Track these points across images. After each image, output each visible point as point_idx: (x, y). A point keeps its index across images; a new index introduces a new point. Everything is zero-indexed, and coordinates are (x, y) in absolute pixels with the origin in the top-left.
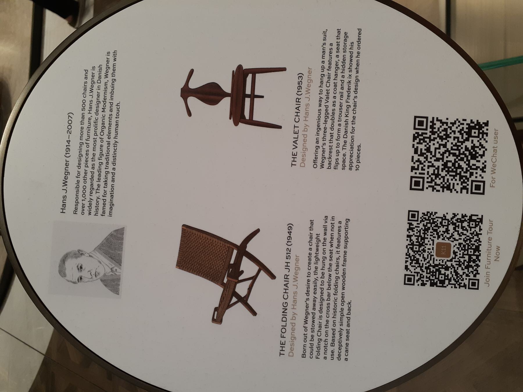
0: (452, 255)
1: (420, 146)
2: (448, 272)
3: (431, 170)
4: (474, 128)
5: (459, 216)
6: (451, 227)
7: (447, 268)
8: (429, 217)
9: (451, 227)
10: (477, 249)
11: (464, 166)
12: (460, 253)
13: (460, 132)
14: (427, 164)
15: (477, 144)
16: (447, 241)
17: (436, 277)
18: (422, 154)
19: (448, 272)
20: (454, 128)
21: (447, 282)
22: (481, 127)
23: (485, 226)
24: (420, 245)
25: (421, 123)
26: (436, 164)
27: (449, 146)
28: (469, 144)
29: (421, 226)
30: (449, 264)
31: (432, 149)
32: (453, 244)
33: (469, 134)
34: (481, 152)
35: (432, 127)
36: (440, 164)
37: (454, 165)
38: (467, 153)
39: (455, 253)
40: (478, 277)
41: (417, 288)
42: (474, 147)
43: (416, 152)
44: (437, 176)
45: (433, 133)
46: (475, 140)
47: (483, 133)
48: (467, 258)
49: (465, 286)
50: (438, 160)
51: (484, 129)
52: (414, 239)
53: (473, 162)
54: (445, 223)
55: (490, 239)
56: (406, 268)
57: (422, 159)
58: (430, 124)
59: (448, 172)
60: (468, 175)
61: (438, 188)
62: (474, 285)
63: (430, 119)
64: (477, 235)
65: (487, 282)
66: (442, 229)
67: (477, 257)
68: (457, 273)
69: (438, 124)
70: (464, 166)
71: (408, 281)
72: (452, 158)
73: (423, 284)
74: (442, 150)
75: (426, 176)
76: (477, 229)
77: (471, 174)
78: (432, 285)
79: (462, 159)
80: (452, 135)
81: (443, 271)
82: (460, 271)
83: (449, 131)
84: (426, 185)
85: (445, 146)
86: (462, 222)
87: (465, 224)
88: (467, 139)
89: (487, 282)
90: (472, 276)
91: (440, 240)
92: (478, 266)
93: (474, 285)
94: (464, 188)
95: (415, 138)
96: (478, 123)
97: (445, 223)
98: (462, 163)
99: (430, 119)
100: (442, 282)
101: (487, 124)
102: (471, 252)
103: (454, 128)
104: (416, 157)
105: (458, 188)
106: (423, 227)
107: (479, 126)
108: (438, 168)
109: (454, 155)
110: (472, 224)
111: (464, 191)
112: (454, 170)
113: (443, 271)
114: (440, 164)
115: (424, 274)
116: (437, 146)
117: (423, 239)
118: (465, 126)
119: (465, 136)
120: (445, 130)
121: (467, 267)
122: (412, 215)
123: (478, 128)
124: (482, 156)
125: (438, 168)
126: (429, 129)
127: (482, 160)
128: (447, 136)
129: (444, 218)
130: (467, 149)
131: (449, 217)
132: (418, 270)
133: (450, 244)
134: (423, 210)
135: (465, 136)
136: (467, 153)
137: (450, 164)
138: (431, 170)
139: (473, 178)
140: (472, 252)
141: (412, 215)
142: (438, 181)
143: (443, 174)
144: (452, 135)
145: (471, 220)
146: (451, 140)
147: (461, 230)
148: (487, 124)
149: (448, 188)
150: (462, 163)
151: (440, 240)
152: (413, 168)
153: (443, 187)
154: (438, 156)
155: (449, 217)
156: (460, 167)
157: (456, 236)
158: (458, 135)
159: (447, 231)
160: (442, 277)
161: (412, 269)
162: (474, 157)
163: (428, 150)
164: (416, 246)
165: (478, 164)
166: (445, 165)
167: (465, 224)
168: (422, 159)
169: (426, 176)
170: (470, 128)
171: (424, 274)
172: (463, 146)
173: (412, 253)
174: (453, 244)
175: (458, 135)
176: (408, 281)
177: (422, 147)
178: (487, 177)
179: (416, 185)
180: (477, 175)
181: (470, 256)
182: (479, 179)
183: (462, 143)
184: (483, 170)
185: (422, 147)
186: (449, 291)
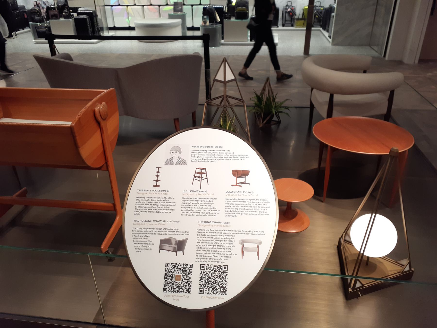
0: (176, 281)
1: (216, 268)
2: (170, 280)
3: (208, 272)
4: (224, 289)
5: (190, 284)
6: (186, 281)
7: (171, 279)
8: (190, 272)
9: (186, 281)
10: (178, 291)
11: (209, 286)
12: (177, 284)
13: (222, 283)
14: (210, 270)
15: (218, 291)
16: (181, 279)
17: (168, 275)
18: (213, 268)
19: (170, 280)
20: (224, 281)
21: (166, 280)
22: (224, 292)
23: (187, 294)
24: (180, 269)
25: (225, 268)
26: (210, 274)
27: (217, 279)
28: (218, 287)
29: (187, 269)
30: (173, 280)
31: (216, 273)
32: (180, 282)
33: (222, 287)
34: (215, 292)
35: (224, 272)
36: (210, 276)
37: (210, 281)
38: (214, 287)
39: (177, 282)
40: (168, 292)
41: (165, 268)
42: (217, 289)
43: (214, 266)
44: (206, 275)
45: (222, 273)
46: (219, 290)
47: (222, 293)
48: (175, 287)
49: (165, 287)
50: (212, 275)
51: (224, 294)
52: (182, 266)
53: (211, 289)
54: (188, 278)
55: (182, 296)
56: (172, 264)
57: (212, 269)
58: (225, 271)
59: (207, 279)
60: (206, 287)
61: (201, 275)
62: (165, 290)
63: (227, 271)
64: (183, 291)
65: (166, 296)
66: (186, 277)
67: (175, 292)
68: (169, 283)
69: (225, 275)
70: (209, 286)
71: (167, 265)
72: (212, 280)
73: (166, 270)
74: (215, 277)
75: (206, 270)
76: (186, 291)
77: (206, 289)
78: (165, 274)
79: (212, 285)
80: (221, 281)
81: (170, 278)
82: (170, 285)
83: (223, 279)
84: (202, 270)
85: (217, 277)
86: (188, 285)
87: (187, 286)
88: (220, 287)
89: (166, 296)
90: (168, 289)
91: (182, 277)
92: (172, 292)
93: (165, 290)
94: (201, 286)
95: (219, 265)
96: (226, 291)
97: (188, 278)
98: (211, 284)
99: (227, 271)
100: (166, 278)
101: (226, 294)
102: (177, 289)
103: (224, 281)
104: (212, 266)
105: (201, 283)
106: (186, 269)
107: (225, 291)
108: (208, 275)
109: (214, 281)
110: (187, 289)
111: (200, 286)
112: (208, 282)
113: (170, 278)
114: (210, 276)
115: (169, 271)
116: (217, 274)
117: (182, 270)
118: (225, 286)
119: (221, 286)
120: (223, 278)
121: (171, 288)
122: (191, 265)
123: (224, 291)
124: (213, 293)
125: (208, 275)
126: (223, 271)
127: (212, 293)
128: (221, 278)
129: (190, 278)
130: (216, 286)
131: (190, 280)
132: (171, 268)
133: (180, 280)
134: (193, 269)
135: (221, 286)
136: (214, 287)
137: (210, 280)
138: (208, 272)
139: (205, 289)
140: (176, 289)
141: (191, 265)
142: (204, 275)
143: (206, 277)
144: (221, 281)
145: (189, 288)
146: (219, 280)
147: (185, 285)
148: (226, 294)
149: (201, 279)
150: (211, 284)
151: (182, 277)
152: (208, 265)
153: (201, 277)
154: (213, 275)
155: (190, 280)
156: (209, 284)
157: (183, 283)
158: (221, 283)
159: (185, 279)
160: (168, 278)
161: (171, 266)
162: (213, 289)
163: (215, 271)
164: (180, 267)
165: (210, 291)
166: (210, 278)
167: (187, 286)
168: (212, 269)
169: (206, 270)
170: (224, 288)
171: (169, 271)
172: (217, 285)
173: (177, 266)
174: (180, 282)
175: (221, 283)
176: (167, 265)
177: (216, 269)
178: (206, 295)
179: (202, 267)
180: (206, 291)
181: (175, 289)
182: (205, 292)
183: (218, 285)
184: (208, 293)
185: (216, 269)
186: (163, 280)
